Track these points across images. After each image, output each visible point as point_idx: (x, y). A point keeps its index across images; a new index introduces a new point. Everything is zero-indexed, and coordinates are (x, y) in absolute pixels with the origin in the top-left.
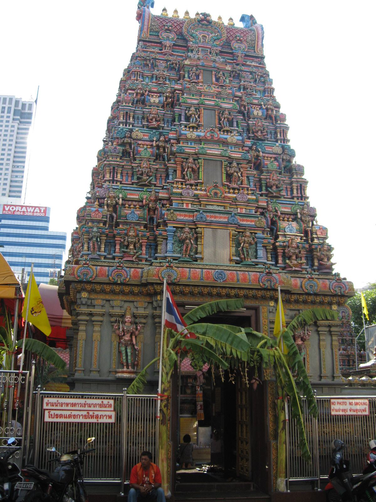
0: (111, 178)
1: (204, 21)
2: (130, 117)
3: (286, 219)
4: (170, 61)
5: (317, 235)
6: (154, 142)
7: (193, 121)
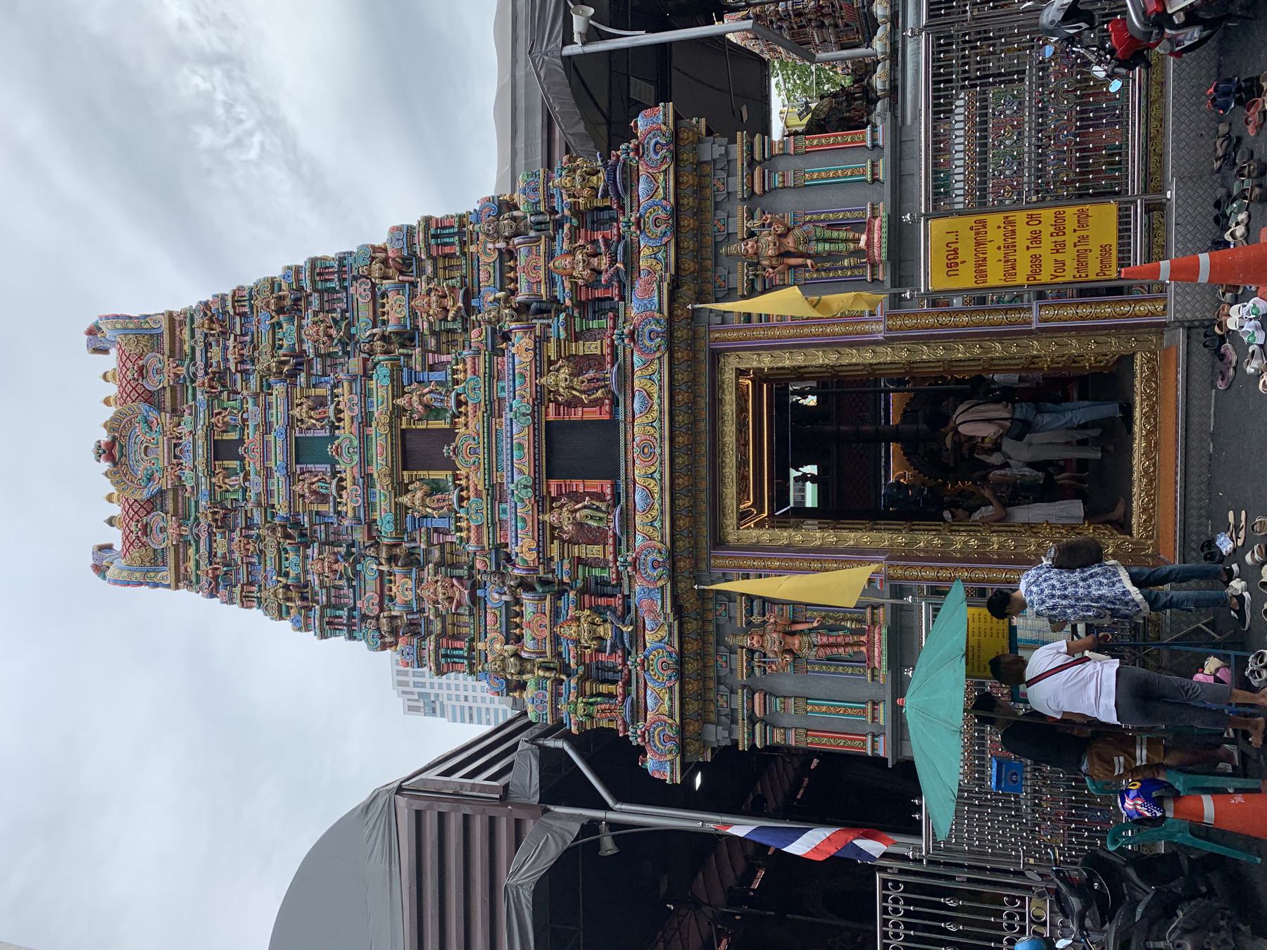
1: (113, 452)
2: (336, 617)
3: (512, 275)
4: (210, 526)
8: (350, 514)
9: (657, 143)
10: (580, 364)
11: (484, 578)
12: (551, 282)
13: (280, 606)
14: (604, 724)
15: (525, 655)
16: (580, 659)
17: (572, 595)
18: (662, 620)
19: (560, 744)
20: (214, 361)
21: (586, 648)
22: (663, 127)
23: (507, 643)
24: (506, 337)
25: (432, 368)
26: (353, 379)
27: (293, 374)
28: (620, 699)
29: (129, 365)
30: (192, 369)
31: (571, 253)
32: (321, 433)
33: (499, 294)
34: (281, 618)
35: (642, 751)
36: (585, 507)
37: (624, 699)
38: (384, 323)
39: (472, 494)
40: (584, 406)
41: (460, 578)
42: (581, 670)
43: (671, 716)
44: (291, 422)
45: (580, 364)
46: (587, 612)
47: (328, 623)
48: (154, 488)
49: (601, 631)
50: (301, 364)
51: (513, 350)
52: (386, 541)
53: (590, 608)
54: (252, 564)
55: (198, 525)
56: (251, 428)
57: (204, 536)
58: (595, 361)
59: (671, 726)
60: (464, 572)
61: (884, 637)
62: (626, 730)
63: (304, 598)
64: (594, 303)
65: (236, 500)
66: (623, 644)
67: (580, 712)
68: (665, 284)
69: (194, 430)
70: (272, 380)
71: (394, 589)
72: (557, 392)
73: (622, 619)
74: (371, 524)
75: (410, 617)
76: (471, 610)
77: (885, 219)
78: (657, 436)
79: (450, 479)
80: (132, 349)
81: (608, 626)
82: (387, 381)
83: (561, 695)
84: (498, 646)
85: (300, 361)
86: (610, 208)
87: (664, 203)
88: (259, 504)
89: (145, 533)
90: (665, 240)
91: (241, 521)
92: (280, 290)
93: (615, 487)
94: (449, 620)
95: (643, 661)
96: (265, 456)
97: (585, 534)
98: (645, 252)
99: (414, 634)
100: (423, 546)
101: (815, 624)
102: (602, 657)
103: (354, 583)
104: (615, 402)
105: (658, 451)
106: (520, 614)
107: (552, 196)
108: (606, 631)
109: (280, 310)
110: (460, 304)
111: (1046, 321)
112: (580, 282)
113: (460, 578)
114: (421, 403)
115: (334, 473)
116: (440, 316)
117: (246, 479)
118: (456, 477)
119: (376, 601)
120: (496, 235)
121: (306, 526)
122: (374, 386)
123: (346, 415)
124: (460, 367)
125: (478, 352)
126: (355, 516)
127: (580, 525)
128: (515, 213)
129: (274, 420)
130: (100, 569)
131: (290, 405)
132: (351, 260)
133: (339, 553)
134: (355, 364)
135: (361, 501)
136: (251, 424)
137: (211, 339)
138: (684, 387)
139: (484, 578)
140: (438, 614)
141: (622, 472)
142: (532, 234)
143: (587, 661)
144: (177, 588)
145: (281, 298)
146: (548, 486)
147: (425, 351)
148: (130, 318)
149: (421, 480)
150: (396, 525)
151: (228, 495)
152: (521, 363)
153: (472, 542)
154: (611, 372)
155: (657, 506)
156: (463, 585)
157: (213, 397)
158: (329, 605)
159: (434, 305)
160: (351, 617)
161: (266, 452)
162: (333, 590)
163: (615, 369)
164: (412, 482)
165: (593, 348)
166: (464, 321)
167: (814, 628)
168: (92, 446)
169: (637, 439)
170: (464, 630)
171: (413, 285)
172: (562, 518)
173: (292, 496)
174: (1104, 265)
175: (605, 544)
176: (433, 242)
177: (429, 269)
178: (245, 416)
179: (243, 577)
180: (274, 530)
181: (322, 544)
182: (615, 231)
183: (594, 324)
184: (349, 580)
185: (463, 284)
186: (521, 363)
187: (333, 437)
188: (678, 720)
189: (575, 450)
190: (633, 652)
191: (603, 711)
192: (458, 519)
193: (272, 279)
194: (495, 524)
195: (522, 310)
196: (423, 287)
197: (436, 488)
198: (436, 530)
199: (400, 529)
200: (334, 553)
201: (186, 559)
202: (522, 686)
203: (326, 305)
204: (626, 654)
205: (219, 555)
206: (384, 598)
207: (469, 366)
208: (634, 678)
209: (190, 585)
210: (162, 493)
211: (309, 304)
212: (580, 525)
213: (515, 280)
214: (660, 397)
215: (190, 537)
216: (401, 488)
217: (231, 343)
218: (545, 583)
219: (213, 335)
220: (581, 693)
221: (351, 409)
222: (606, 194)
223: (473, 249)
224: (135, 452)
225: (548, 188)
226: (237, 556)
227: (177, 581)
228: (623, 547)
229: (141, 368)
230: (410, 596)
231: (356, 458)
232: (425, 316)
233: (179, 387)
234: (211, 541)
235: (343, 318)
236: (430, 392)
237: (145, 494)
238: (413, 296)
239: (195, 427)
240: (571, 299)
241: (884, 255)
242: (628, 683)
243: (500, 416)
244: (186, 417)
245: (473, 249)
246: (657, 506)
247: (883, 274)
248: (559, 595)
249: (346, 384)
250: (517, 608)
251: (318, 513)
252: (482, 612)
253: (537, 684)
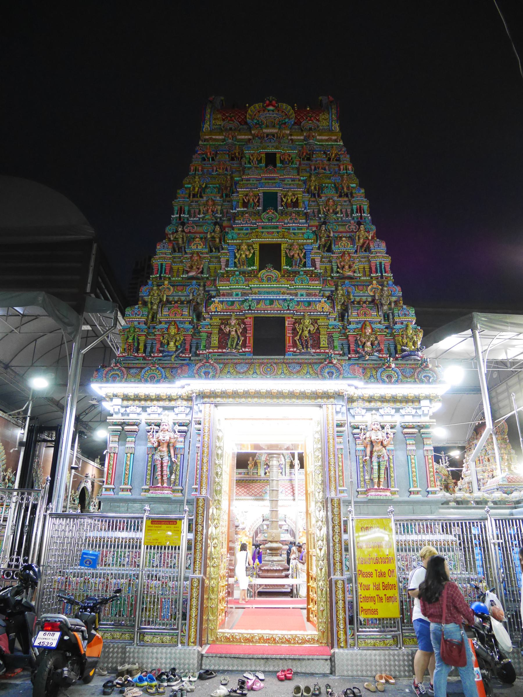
28: (136, 354)
40: (293, 337)
61: (166, 496)
77: (390, 498)
101: (173, 459)
111: (336, 584)
167: (171, 459)
174: (366, 611)
175: (219, 348)
182: (384, 356)
241: (372, 497)
242: (144, 358)
247: (361, 498)
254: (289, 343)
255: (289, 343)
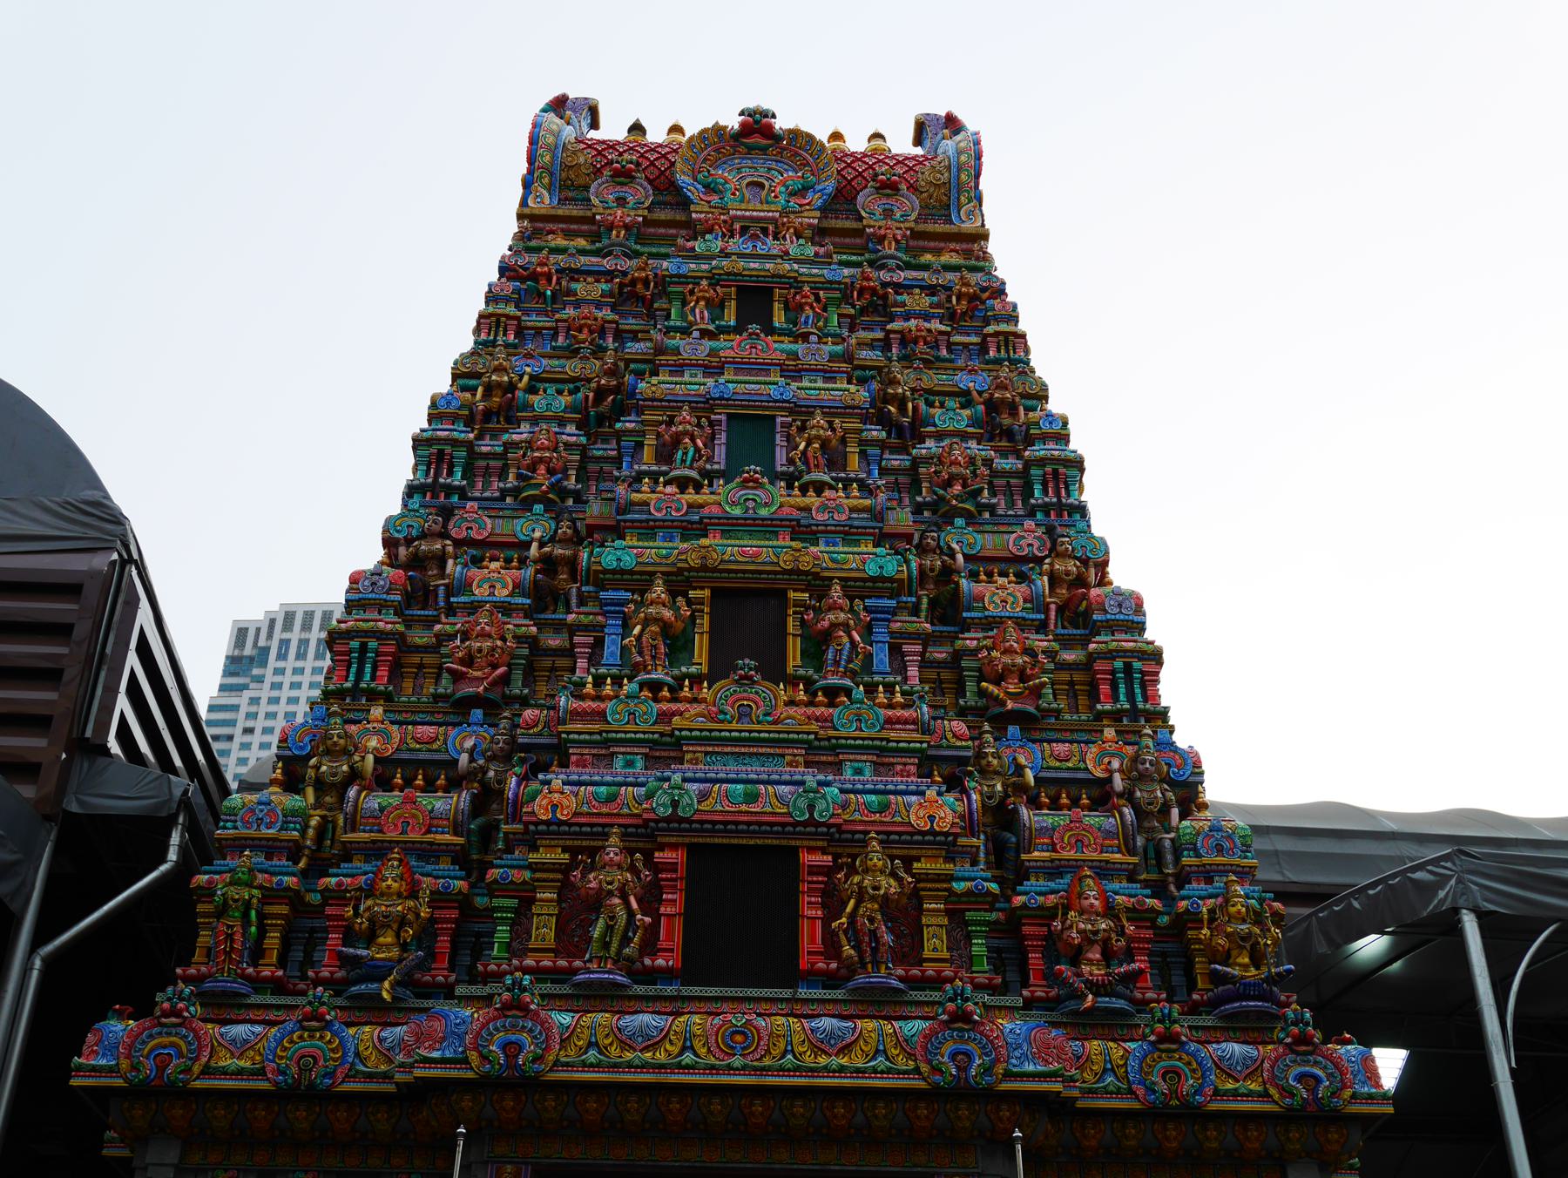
0: (348, 685)
3: (1064, 800)
4: (625, 274)
5: (1198, 856)
6: (535, 545)
7: (683, 461)
8: (636, 497)
9: (1318, 1080)
10: (904, 915)
11: (504, 723)
12: (1054, 870)
13: (478, 376)
14: (204, 938)
15: (352, 792)
16: (336, 896)
17: (459, 884)
18: (400, 1058)
19: (172, 855)
20: (905, 297)
21: (356, 908)
22: (1347, 1093)
23: (377, 760)
24: (954, 783)
25: (895, 651)
26: (878, 515)
27: (883, 420)
29: (900, 170)
30: (892, 262)
31: (1109, 910)
32: (780, 456)
33: (1030, 776)
34: (455, 377)
35: (142, 1009)
36: (631, 914)
37: (247, 978)
38: (973, 576)
39: (665, 706)
40: (826, 922)
41: (505, 680)
42: (315, 898)
43: (207, 1071)
44: (800, 411)
45: (904, 915)
46: (425, 912)
47: (441, 452)
48: (694, 191)
49: (387, 938)
50: (900, 435)
51: (931, 793)
52: (585, 555)
53: (432, 920)
54: (555, 337)
55: (626, 255)
56: (793, 347)
57: (607, 264)
58: (909, 950)
59: (188, 1071)
60: (517, 688)
62: (187, 980)
63: (488, 415)
64: (1022, 951)
65: (668, 317)
66: (355, 983)
67: (233, 892)
68: (1058, 1087)
69: (793, 256)
70: (875, 386)
71: (494, 565)
72: (853, 871)
73: (406, 982)
74: (618, 531)
75: (442, 590)
76: (444, 698)
78: (767, 1062)
79: (693, 669)
80: (926, 176)
81: (395, 953)
82: (872, 569)
83: (269, 857)
84: (373, 743)
85: (909, 433)
86: (1192, 986)
87: (1209, 1091)
88: (660, 350)
89: (617, 174)
90: (1141, 1092)
91: (631, 323)
92: (1028, 409)
93: (667, 975)
94: (429, 659)
95: (320, 1018)
96: (742, 366)
97: (579, 910)
98: (1116, 1052)
99: (409, 599)
100: (571, 617)
102: (334, 938)
103: (509, 500)
104: (830, 980)
105: (737, 1061)
106: (430, 787)
107: (1209, 881)
108: (385, 948)
109: (992, 406)
110: (1010, 705)
112: (1057, 924)
113: (505, 680)
114: (834, 626)
115: (710, 476)
116: (987, 670)
117: (705, 334)
118: (696, 680)
119: (473, 534)
120: (1137, 774)
121: (618, 425)
122: (863, 549)
123: (812, 499)
124: (899, 698)
125: (926, 730)
126: (633, 504)
127: (596, 902)
128: (1175, 812)
129: (806, 384)
130: (559, 105)
131: (831, 412)
132: (1081, 525)
133: (567, 477)
134: (901, 518)
135: (659, 515)
136: (799, 348)
137: (943, 297)
138: (859, 1118)
139: (504, 723)
140: (442, 639)
141: (696, 991)
142: (1140, 841)
143: (329, 910)
144: (520, 217)
145: (1013, 409)
146: (674, 847)
147: (926, 640)
148: (978, 176)
149: (693, 618)
150: (614, 572)
151: (677, 304)
152: (908, 806)
153: (576, 704)
154: (890, 975)
155: (629, 1056)
156: (493, 684)
157: (845, 292)
158: (473, 455)
159: (1007, 659)
160: (449, 490)
161: (753, 368)
162: (499, 463)
163: (895, 983)
164: (689, 603)
165: (935, 944)
166: (980, 712)
168: (766, 105)
169: (761, 1022)
170: (408, 684)
171: (1042, 627)
172: (612, 871)
173: (671, 406)
175: (556, 952)
176: (1119, 664)
177: (1069, 656)
178: (813, 338)
179: (534, 320)
180: (612, 372)
181: (584, 450)
182: (1150, 995)
183: (979, 947)
184: (515, 492)
185: (1047, 713)
186: (908, 806)
187: (775, 477)
188: (198, 1084)
189: (741, 903)
190: (339, 1001)
191: (230, 937)
192: (617, 681)
193: (1046, 398)
194: (605, 748)
195: (1001, 817)
196: (1039, 642)
197: (677, 643)
198: (599, 643)
199: (603, 579)
200: (565, 471)
201: (569, 235)
202: (292, 783)
203: (1003, 481)
204: (337, 987)
205: (574, 285)
206: (479, 550)
207: (899, 713)
208: (289, 1000)
209: (521, 236)
210: (685, 203)
211: (1003, 453)
212: (596, 902)
213: (1055, 805)
214: (842, 1069)
215: (605, 241)
216: (679, 582)
217: (936, 325)
218: (488, 834)
219: (950, 297)
220: (270, 895)
221: (823, 508)
222: (1217, 979)
223: (1109, 733)
224: (754, 169)
225: (1225, 873)
226: (570, 312)
227: (533, 218)
228: (548, 988)
229: (894, 187)
230: (481, 592)
231: (737, 512)
232: (988, 642)
233: (863, 242)
234: (599, 275)
235: (981, 508)
236: (852, 642)
237: (683, 179)
238: (1021, 624)
239: (797, 261)
240: (1024, 906)
242: (279, 987)
243: (808, 764)
244: (810, 250)
245: (1109, 733)
246: (629, 1056)
248: (460, 857)
249: (867, 502)
250: (441, 782)
251: (640, 445)
252: (440, 718)
253: (294, 813)
254: (813, 940)
255: (813, 940)
